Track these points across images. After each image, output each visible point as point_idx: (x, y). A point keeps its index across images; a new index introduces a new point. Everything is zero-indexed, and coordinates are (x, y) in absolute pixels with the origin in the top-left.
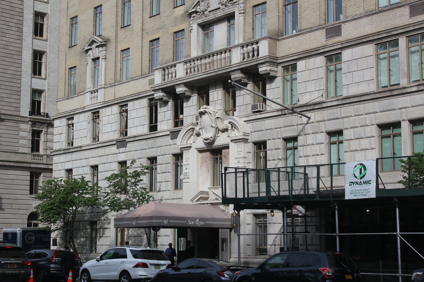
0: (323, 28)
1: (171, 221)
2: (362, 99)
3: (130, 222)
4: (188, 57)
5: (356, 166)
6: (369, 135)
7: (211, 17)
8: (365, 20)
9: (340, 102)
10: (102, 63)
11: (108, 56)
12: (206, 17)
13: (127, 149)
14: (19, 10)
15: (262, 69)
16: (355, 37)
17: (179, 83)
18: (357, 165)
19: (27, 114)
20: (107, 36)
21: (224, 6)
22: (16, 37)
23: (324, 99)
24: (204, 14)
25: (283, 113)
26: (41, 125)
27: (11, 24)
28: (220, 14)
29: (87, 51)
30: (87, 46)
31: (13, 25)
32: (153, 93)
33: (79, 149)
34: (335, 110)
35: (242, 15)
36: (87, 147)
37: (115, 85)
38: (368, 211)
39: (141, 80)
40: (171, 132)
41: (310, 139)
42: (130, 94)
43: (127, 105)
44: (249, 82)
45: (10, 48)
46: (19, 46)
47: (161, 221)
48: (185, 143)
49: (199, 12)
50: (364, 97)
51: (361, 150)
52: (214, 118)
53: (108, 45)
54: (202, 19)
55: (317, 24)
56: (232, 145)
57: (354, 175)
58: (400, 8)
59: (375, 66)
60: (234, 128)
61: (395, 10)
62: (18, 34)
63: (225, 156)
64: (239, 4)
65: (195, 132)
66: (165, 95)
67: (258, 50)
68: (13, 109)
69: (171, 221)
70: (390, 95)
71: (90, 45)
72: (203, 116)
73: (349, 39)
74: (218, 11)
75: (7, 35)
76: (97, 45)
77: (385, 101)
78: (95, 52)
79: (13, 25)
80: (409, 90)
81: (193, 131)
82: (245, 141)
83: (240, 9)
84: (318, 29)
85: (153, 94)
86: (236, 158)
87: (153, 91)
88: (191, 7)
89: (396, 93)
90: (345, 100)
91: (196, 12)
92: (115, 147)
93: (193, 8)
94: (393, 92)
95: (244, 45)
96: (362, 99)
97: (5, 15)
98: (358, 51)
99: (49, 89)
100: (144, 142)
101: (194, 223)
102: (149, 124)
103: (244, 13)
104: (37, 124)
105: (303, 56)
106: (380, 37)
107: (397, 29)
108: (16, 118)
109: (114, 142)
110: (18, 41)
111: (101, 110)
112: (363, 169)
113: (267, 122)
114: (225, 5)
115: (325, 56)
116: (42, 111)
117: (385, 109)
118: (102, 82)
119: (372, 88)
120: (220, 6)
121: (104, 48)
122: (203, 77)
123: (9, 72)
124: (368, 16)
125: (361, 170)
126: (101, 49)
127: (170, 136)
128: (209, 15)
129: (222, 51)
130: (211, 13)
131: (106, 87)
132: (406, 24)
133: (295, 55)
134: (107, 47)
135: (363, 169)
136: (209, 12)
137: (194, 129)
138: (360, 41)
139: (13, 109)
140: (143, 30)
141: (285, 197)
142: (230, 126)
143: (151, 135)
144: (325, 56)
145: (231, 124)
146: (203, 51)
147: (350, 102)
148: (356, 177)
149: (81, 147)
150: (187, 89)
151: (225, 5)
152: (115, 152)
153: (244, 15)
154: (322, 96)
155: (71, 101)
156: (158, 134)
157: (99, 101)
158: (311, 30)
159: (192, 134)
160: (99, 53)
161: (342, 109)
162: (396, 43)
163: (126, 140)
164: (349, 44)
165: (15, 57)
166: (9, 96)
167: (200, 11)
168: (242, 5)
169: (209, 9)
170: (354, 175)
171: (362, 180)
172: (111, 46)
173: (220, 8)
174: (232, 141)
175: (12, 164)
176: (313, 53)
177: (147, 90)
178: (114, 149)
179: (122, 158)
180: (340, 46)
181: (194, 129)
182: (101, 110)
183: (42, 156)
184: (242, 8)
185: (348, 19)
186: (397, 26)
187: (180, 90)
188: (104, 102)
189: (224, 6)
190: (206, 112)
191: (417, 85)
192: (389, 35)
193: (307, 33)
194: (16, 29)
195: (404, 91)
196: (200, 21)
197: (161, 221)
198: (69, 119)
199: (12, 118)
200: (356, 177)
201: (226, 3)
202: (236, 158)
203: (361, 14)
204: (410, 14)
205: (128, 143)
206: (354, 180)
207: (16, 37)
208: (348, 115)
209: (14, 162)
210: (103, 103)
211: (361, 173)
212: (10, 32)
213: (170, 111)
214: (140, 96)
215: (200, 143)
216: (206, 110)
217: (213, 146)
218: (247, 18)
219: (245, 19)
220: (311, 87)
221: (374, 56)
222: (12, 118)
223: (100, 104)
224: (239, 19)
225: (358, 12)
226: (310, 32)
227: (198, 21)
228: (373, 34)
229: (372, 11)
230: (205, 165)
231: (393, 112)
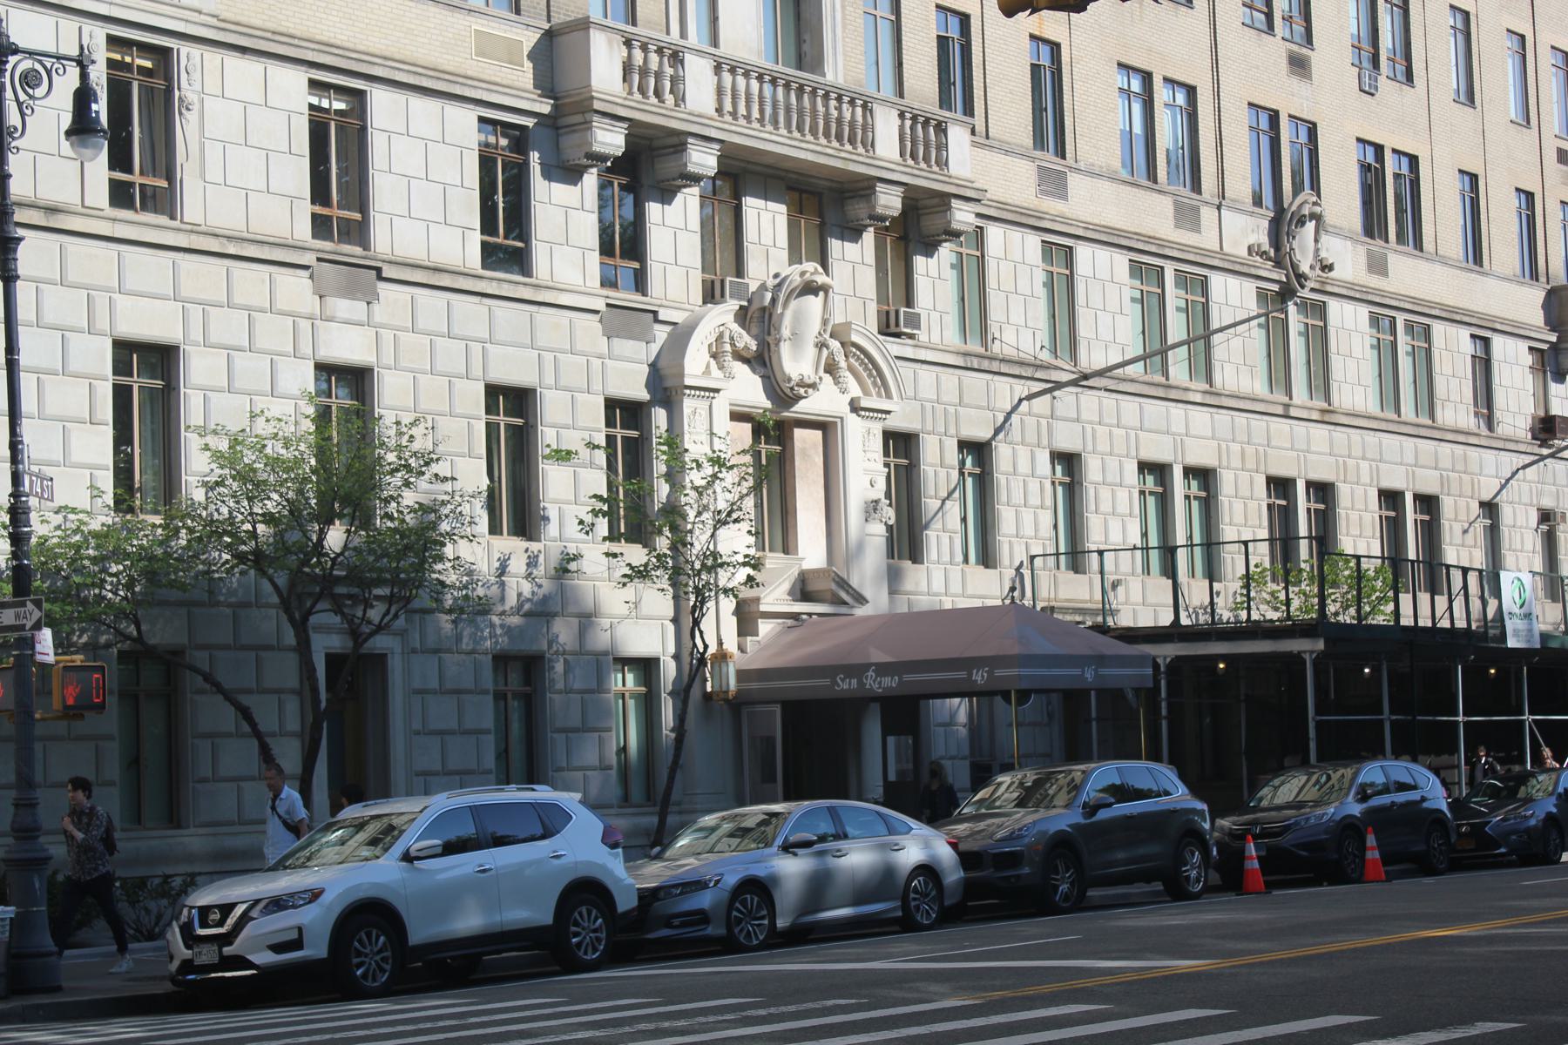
3: (1076, 672)
36: (110, 224)
40: (608, 305)
47: (963, 674)
69: (998, 673)
95: (909, 110)
127: (597, 317)
129: (651, 42)
133: (994, 204)
141: (1425, 629)
143: (521, 288)
144: (1043, 241)
149: (52, 210)
152: (306, 310)
154: (1042, 347)
156: (555, 293)
178: (295, 289)
179: (348, 348)
180: (1080, 232)
185: (1082, 165)
191: (1205, 392)
197: (963, 674)
210: (214, 22)
214: (458, 90)
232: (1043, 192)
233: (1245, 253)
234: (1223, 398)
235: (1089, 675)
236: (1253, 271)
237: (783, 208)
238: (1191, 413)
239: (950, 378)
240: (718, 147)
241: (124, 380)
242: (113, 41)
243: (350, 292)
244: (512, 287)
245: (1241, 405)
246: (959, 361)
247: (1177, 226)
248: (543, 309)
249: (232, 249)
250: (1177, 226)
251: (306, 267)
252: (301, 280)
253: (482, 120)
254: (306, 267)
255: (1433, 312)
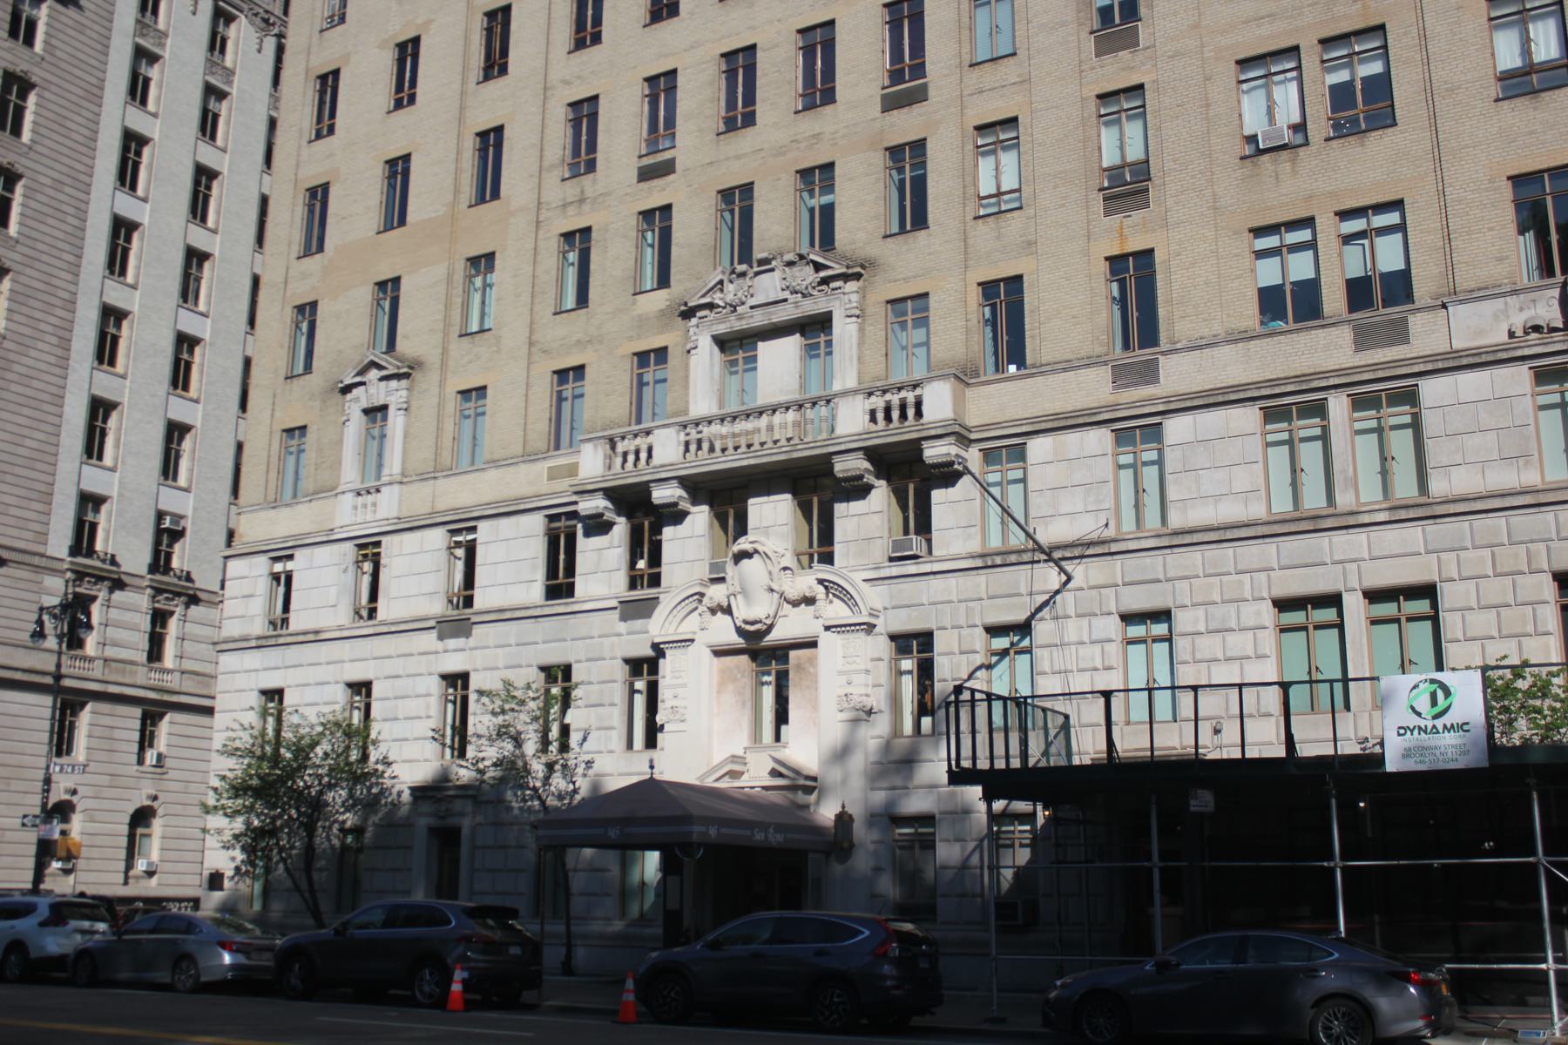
0: (1105, 363)
1: (724, 830)
2: (1229, 535)
4: (677, 416)
5: (1415, 687)
6: (1251, 623)
7: (758, 320)
8: (1227, 349)
9: (1165, 542)
10: (396, 422)
11: (414, 404)
12: (740, 319)
13: (472, 642)
14: (66, 296)
15: (934, 452)
16: (1201, 389)
17: (664, 475)
18: (1421, 684)
19: (63, 552)
20: (415, 355)
21: (800, 295)
22: (53, 360)
23: (1110, 533)
24: (735, 310)
25: (990, 563)
26: (95, 584)
27: (43, 326)
28: (785, 314)
29: (346, 390)
30: (353, 374)
31: (50, 329)
32: (574, 498)
33: (311, 637)
34: (1148, 560)
35: (854, 319)
37: (435, 478)
38: (1362, 805)
39: (523, 467)
41: (1073, 629)
42: (488, 502)
43: (473, 529)
44: (877, 483)
45: (35, 384)
46: (60, 381)
48: (672, 630)
49: (719, 306)
50: (1235, 530)
51: (1228, 659)
52: (775, 570)
53: (416, 375)
54: (728, 325)
55: (1083, 354)
56: (826, 639)
57: (1413, 708)
58: (1326, 330)
59: (1260, 459)
60: (834, 595)
61: (1313, 332)
62: (59, 352)
63: (799, 667)
64: (844, 294)
65: (705, 600)
66: (611, 506)
67: (650, 450)
68: (30, 536)
70: (1311, 528)
71: (361, 373)
72: (745, 562)
73: (1181, 392)
74: (781, 307)
75: (33, 353)
76: (384, 373)
77: (1295, 544)
78: (376, 391)
79: (50, 329)
80: (1366, 519)
81: (700, 601)
82: (870, 628)
83: (847, 306)
84: (1088, 366)
85: (575, 503)
86: (841, 673)
87: (576, 493)
88: (696, 294)
89: (1329, 523)
90: (1180, 536)
91: (711, 306)
92: (433, 634)
93: (704, 296)
94: (1319, 520)
96: (1229, 535)
97: (32, 303)
98: (1471, 383)
99: (120, 495)
100: (532, 625)
101: (766, 837)
102: (544, 579)
103: (858, 317)
104: (87, 579)
105: (1049, 425)
106: (1277, 391)
107: (1327, 375)
108: (36, 560)
109: (432, 623)
110: (57, 371)
111: (385, 540)
112: (1440, 694)
113: (936, 583)
114: (802, 293)
115: (1112, 431)
116: (99, 546)
117: (1296, 562)
118: (394, 464)
119: (1257, 511)
120: (786, 294)
121: (404, 383)
122: (745, 463)
123: (28, 442)
124: (1236, 341)
125: (1433, 696)
126: (394, 384)
127: (617, 611)
128: (752, 317)
130: (757, 312)
131: (405, 480)
132: (1343, 366)
133: (1025, 422)
134: (413, 380)
135: (1440, 694)
136: (752, 307)
137: (702, 595)
138: (1220, 399)
139: (30, 536)
140: (531, 344)
142: (821, 589)
144: (1112, 431)
145: (826, 588)
146: (721, 405)
147: (1195, 541)
148: (1419, 714)
149: (317, 632)
150: (684, 494)
151: (802, 293)
152: (433, 649)
153: (859, 320)
154: (1107, 525)
155: (284, 513)
157: (378, 517)
158: (1067, 366)
159: (696, 609)
160: (386, 396)
161: (1169, 559)
162: (1318, 410)
163: (469, 619)
164: (1188, 404)
165: (46, 407)
166: (24, 503)
167: (721, 304)
168: (854, 297)
169: (752, 302)
170: (1413, 708)
171: (1439, 723)
172: (427, 381)
173: (786, 300)
174: (827, 628)
175: (18, 676)
176: (1081, 421)
177: (543, 492)
179: (454, 664)
180: (1161, 408)
181: (702, 595)
182: (385, 540)
183: (91, 660)
184: (855, 305)
185: (1179, 346)
186: (1318, 370)
187: (660, 495)
188: (399, 519)
189: (800, 295)
190: (756, 551)
192: (1304, 388)
193: (1054, 371)
194: (54, 340)
195: (1351, 521)
196: (721, 329)
198: (276, 559)
199: (27, 559)
200: (1419, 714)
201: (807, 288)
202: (841, 673)
203: (1215, 336)
204: (1355, 343)
205: (475, 626)
206: (1414, 721)
207: (53, 360)
208: (1186, 573)
209: (24, 671)
210: (396, 521)
211: (1434, 703)
212: (40, 345)
213: (619, 549)
214: (522, 507)
215: (724, 632)
216: (755, 546)
217: (766, 639)
218: (868, 329)
219: (861, 330)
220: (1071, 502)
221: (1259, 435)
222: (27, 559)
223: (386, 522)
224: (844, 330)
225: (1206, 332)
226: (1065, 370)
227: (714, 327)
228: (1258, 385)
229: (1246, 331)
230: (731, 687)
231: (1320, 569)
232: (1119, 387)
233: (1504, 338)
234: (1435, 507)
235: (713, 832)
236: (1519, 353)
237: (788, 496)
238: (1372, 534)
239: (981, 579)
240: (675, 481)
241: (464, 692)
242: (361, 547)
243: (456, 635)
244: (550, 608)
245: (1479, 506)
246: (979, 563)
247: (1357, 351)
248: (1176, 550)
249: (393, 629)
250: (1357, 351)
251: (433, 628)
252: (433, 634)
253: (546, 516)
254: (433, 628)
255: (1416, 369)
